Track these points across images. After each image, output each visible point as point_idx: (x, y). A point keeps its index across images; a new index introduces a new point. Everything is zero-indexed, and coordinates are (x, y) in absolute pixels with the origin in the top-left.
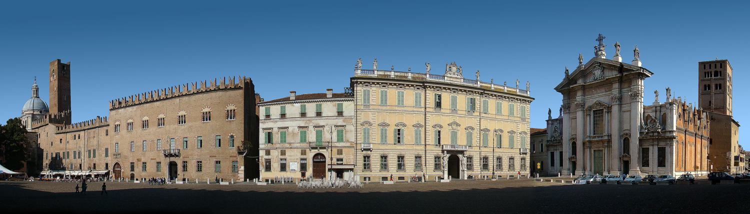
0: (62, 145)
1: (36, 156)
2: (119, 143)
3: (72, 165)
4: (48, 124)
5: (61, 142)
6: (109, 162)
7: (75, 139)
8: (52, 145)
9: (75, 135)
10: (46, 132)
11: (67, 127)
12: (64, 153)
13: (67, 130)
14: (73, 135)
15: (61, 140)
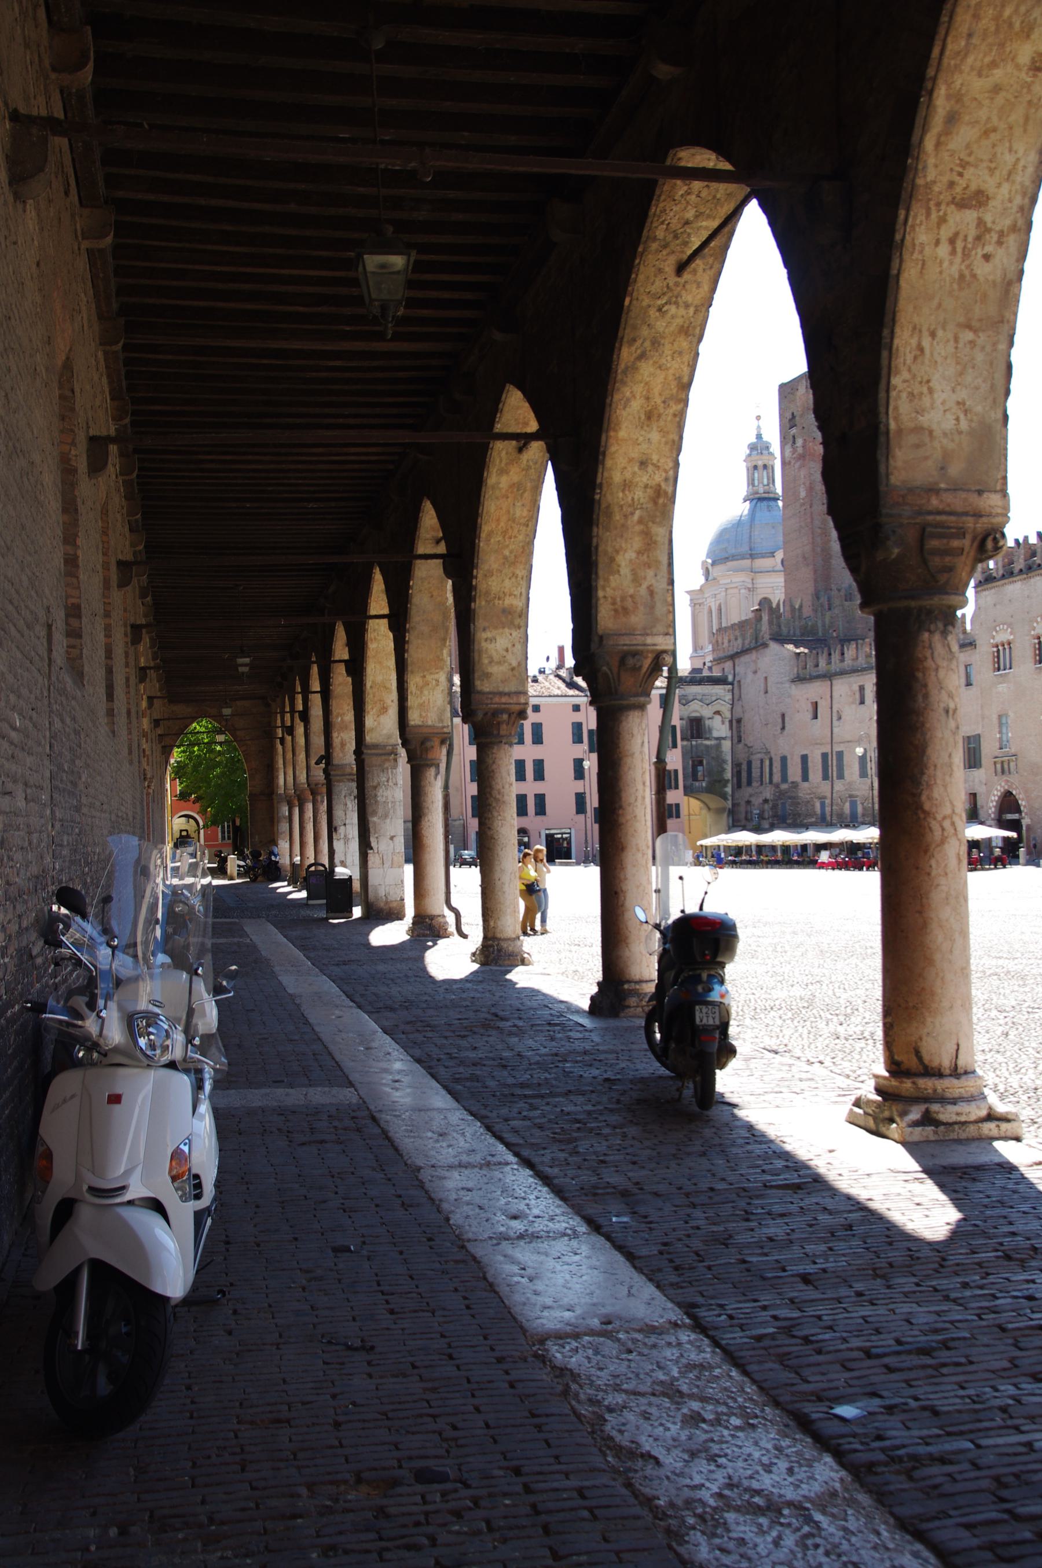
0: (819, 729)
1: (728, 775)
2: (1011, 714)
3: (853, 804)
4: (765, 645)
5: (816, 717)
6: (981, 790)
7: (862, 702)
8: (783, 728)
9: (862, 689)
10: (761, 675)
11: (836, 656)
12: (825, 756)
13: (836, 665)
14: (856, 688)
15: (815, 705)
